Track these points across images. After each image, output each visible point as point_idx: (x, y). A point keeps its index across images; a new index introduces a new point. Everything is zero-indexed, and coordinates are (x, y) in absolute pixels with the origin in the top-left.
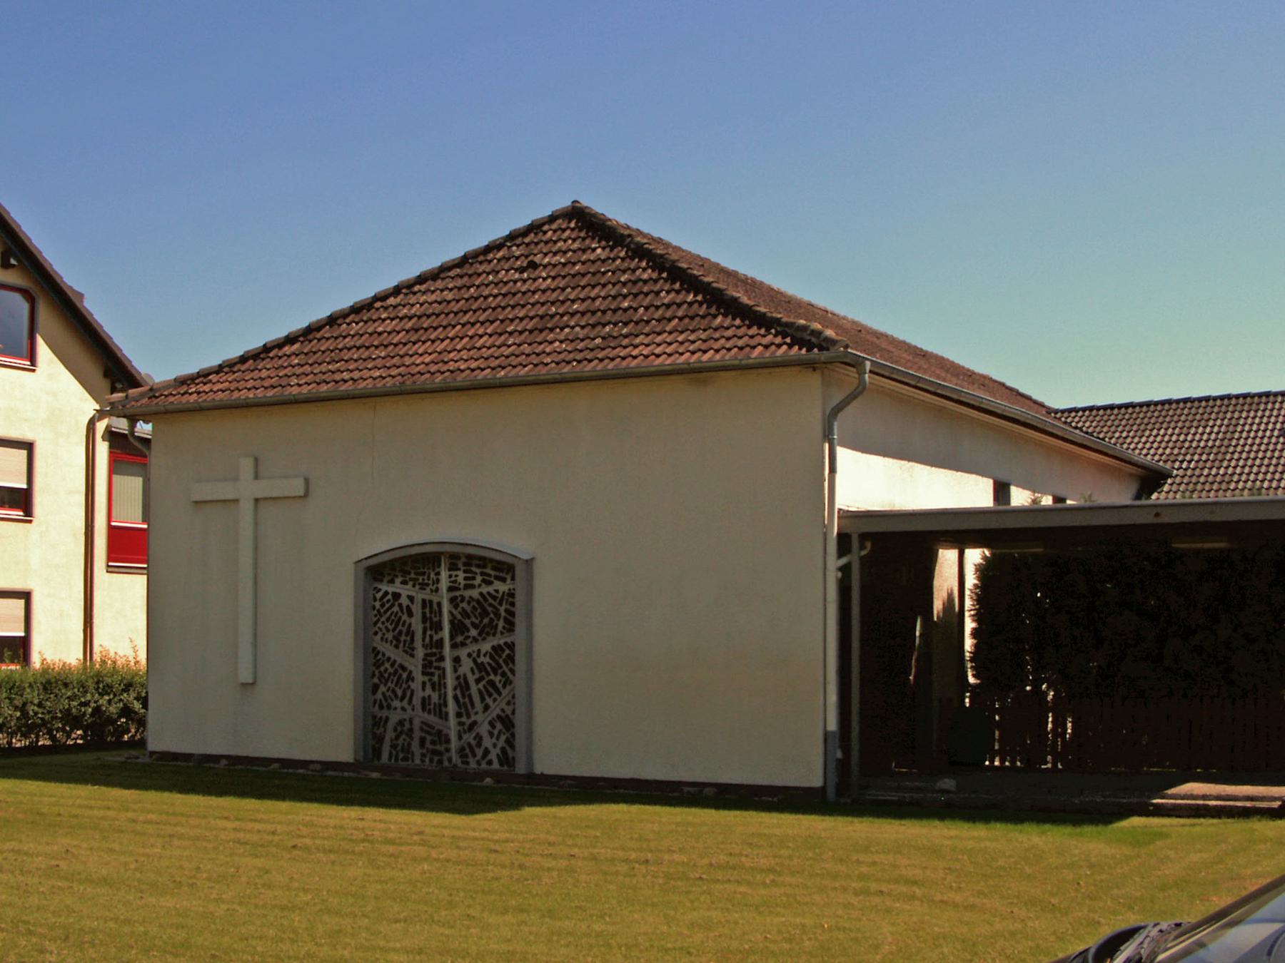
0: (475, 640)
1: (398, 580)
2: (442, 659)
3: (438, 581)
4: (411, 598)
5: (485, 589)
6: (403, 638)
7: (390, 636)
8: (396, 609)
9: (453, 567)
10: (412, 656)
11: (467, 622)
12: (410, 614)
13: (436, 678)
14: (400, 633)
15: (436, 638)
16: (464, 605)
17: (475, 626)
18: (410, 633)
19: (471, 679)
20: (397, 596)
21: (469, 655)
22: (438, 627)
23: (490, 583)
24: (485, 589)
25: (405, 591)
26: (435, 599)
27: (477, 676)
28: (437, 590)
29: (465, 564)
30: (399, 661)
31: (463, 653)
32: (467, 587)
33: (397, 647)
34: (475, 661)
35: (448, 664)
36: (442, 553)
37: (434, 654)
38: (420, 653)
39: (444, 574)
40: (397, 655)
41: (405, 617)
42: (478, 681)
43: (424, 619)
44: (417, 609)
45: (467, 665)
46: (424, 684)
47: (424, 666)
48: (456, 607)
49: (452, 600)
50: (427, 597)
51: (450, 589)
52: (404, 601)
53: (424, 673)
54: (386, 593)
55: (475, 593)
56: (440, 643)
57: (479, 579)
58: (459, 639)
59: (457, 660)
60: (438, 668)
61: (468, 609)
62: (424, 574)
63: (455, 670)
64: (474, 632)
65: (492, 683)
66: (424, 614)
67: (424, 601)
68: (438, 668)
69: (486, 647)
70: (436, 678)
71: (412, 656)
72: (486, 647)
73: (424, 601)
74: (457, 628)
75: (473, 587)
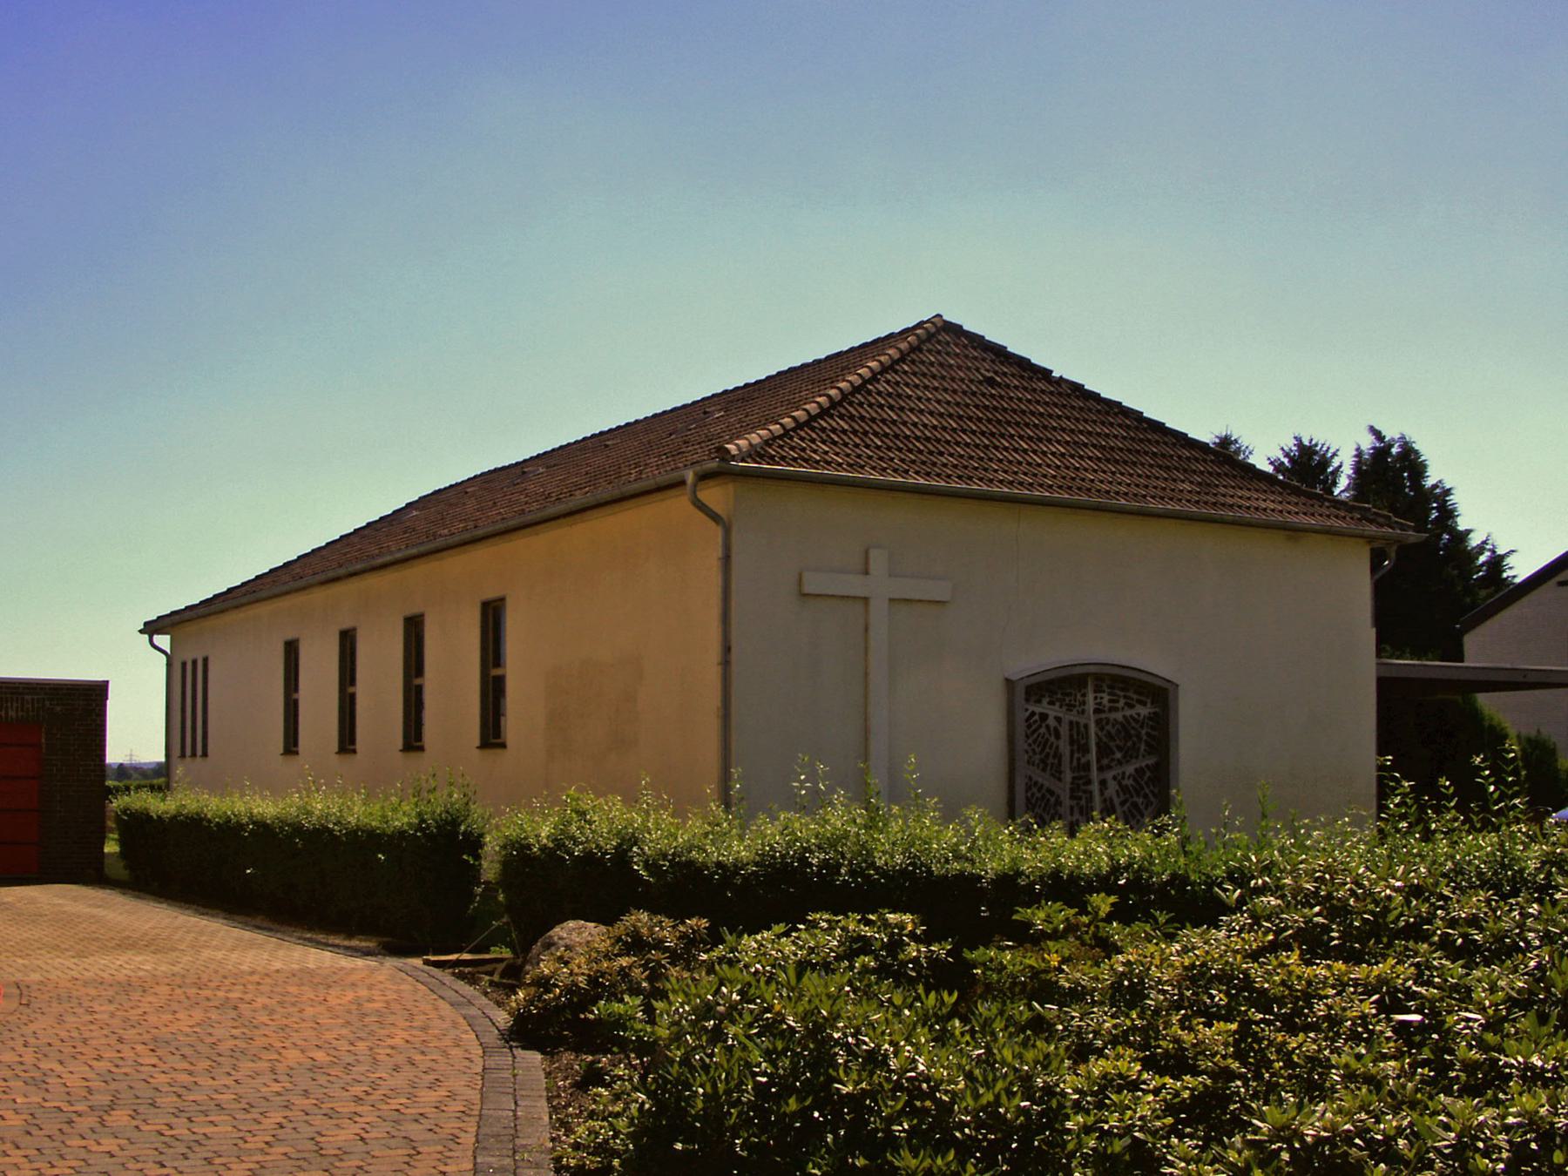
0: (1120, 763)
1: (1045, 701)
2: (1089, 782)
3: (1084, 703)
4: (1058, 720)
5: (1128, 712)
6: (1051, 760)
7: (1037, 758)
8: (1043, 730)
9: (1097, 690)
10: (1060, 779)
11: (1112, 744)
12: (1058, 736)
13: (1083, 802)
14: (1048, 755)
15: (1083, 760)
16: (1109, 727)
17: (1120, 748)
18: (1057, 755)
19: (1116, 801)
20: (1044, 717)
21: (1114, 778)
22: (1085, 750)
23: (1131, 706)
24: (1128, 712)
25: (1053, 712)
26: (1082, 721)
27: (1122, 797)
28: (1083, 712)
29: (1110, 687)
30: (1047, 784)
31: (1109, 775)
32: (1111, 709)
33: (1044, 770)
34: (1120, 784)
35: (1095, 787)
36: (1088, 675)
37: (1081, 778)
38: (1068, 776)
39: (1090, 697)
40: (1046, 780)
41: (1052, 739)
42: (1123, 803)
43: (1072, 742)
44: (1064, 730)
45: (1112, 787)
46: (1072, 808)
47: (1072, 790)
48: (1102, 729)
49: (1098, 722)
50: (1074, 719)
51: (1097, 711)
52: (1051, 722)
53: (1072, 797)
54: (1033, 714)
55: (1119, 716)
56: (1087, 767)
57: (1122, 701)
58: (1105, 762)
59: (1103, 783)
60: (1085, 792)
61: (1113, 732)
62: (1069, 694)
63: (1102, 794)
64: (1118, 755)
65: (1135, 805)
66: (1071, 736)
67: (1071, 723)
68: (1085, 792)
69: (1130, 769)
70: (1083, 802)
71: (1060, 779)
72: (1130, 769)
73: (1071, 723)
74: (1104, 750)
75: (1116, 709)
